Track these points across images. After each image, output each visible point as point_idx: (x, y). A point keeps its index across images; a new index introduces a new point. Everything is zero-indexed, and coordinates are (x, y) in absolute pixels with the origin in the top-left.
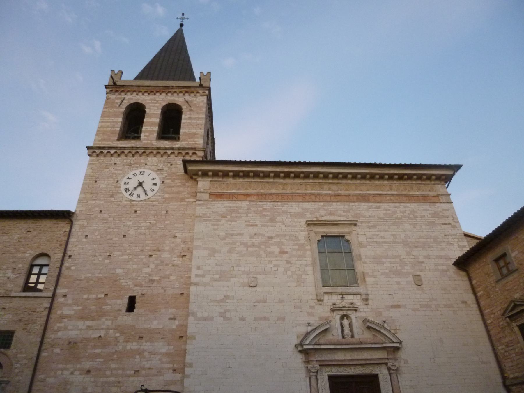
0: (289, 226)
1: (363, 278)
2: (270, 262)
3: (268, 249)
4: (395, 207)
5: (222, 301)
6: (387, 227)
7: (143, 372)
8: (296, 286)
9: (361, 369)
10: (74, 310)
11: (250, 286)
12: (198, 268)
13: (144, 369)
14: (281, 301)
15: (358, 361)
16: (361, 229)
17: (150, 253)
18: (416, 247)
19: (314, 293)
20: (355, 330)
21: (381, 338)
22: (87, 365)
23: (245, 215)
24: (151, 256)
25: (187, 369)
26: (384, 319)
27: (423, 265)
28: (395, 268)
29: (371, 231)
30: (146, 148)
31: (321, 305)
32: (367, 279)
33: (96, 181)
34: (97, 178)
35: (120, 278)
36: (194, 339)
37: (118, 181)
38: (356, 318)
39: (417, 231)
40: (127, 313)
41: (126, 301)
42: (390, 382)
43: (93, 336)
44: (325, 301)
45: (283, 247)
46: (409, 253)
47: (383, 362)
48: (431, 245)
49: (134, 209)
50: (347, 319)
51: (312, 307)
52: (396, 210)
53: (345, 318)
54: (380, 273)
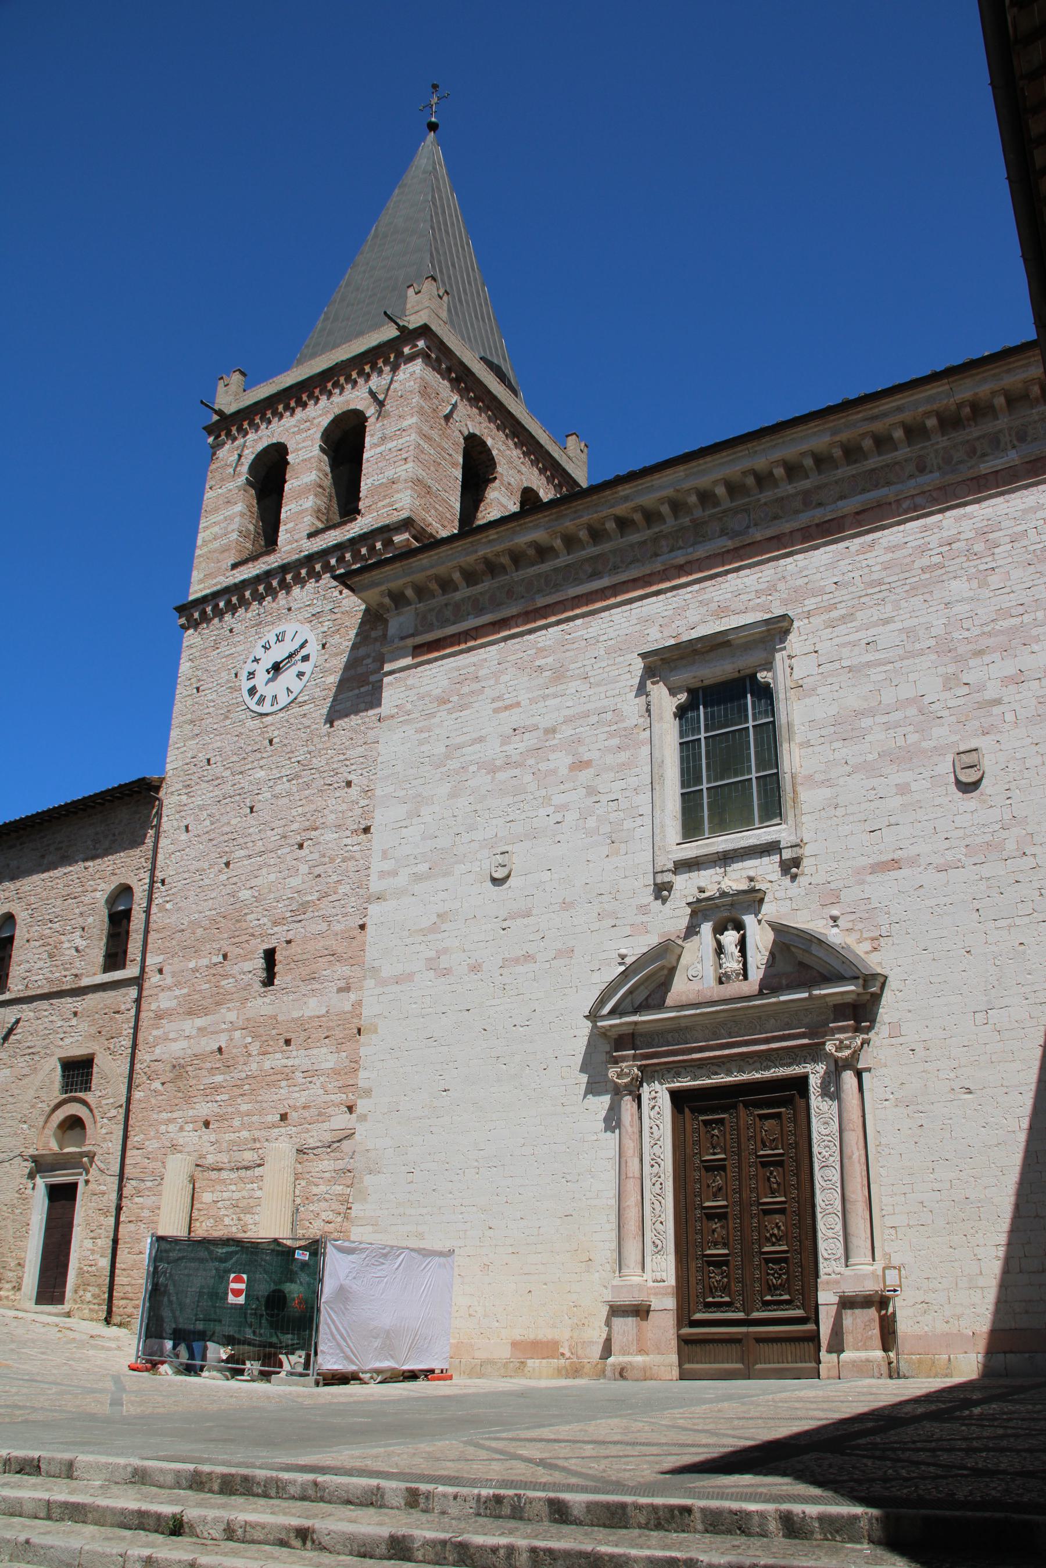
0: (598, 685)
2: (547, 800)
3: (543, 766)
4: (925, 529)
5: (434, 928)
6: (889, 607)
7: (293, 1116)
10: (176, 997)
12: (385, 855)
13: (295, 1108)
14: (566, 905)
16: (805, 637)
17: (299, 839)
18: (980, 653)
22: (204, 1109)
23: (492, 682)
24: (301, 846)
25: (359, 1102)
27: (996, 710)
28: (900, 741)
29: (835, 634)
30: (284, 569)
33: (198, 689)
34: (199, 681)
35: (246, 911)
36: (375, 1032)
37: (236, 675)
39: (992, 594)
40: (264, 989)
41: (260, 963)
43: (208, 1049)
45: (581, 750)
46: (949, 682)
48: (1034, 632)
49: (266, 735)
51: (643, 909)
52: (927, 539)
54: (848, 769)
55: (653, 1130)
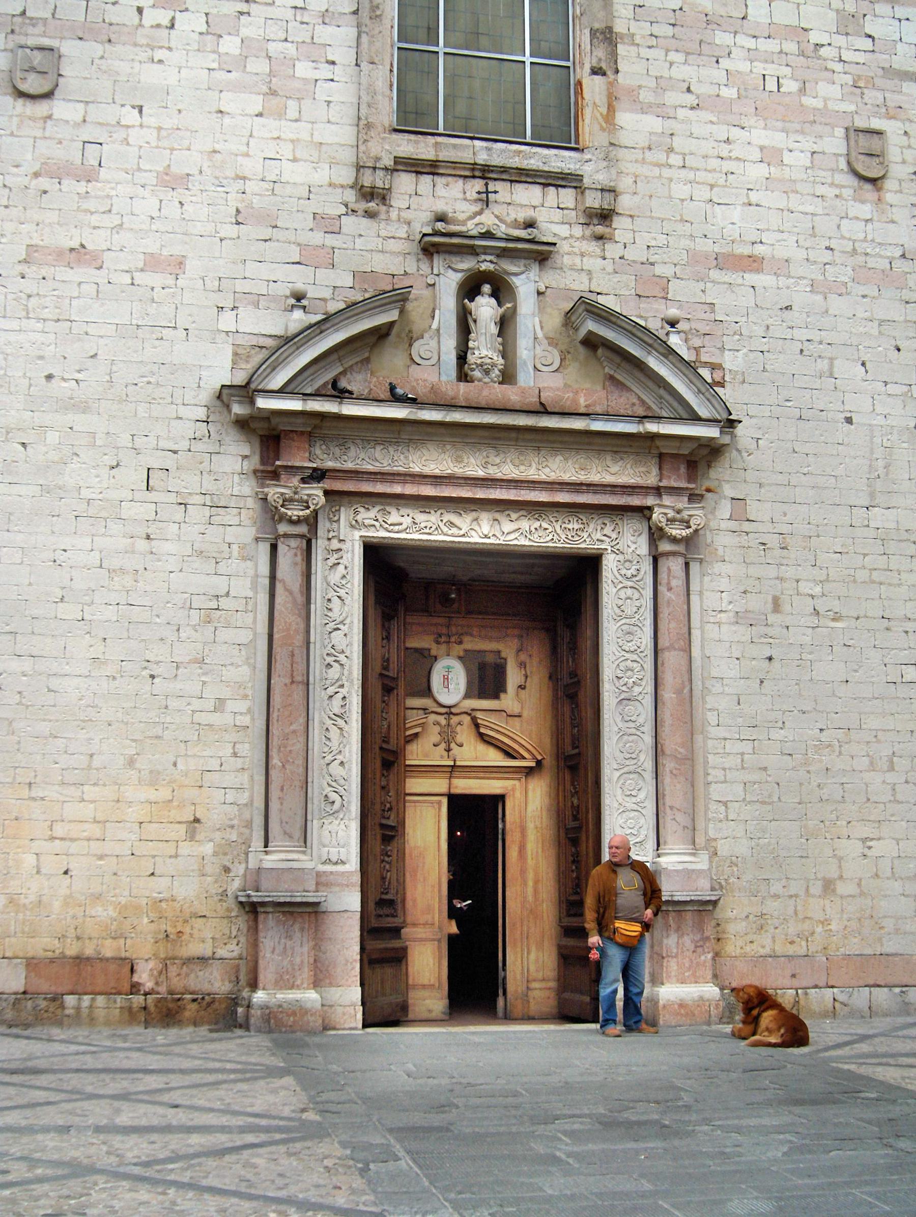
1: (604, 110)
8: (260, 115)
9: (525, 524)
11: (22, 95)
15: (516, 488)
19: (348, 156)
20: (524, 350)
21: (644, 397)
26: (673, 312)
31: (370, 215)
32: (624, 118)
38: (539, 293)
42: (649, 593)
44: (398, 201)
47: (635, 501)
50: (495, 294)
53: (486, 288)
54: (690, 99)
55: (331, 606)
